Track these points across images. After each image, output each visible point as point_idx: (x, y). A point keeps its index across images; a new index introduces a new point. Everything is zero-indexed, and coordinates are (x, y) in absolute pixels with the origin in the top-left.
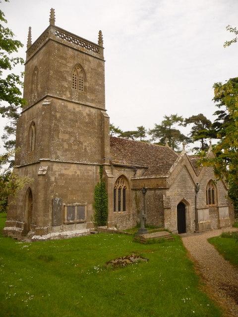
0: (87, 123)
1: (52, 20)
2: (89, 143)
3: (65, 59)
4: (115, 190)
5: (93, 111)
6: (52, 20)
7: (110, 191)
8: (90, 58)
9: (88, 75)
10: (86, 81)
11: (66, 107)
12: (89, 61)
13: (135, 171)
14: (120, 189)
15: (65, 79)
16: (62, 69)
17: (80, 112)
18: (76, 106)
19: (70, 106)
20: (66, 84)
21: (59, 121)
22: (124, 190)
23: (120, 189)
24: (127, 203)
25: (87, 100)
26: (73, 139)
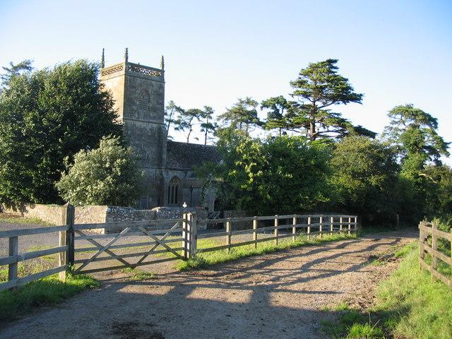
0: (150, 136)
1: (127, 58)
2: (151, 152)
3: (134, 87)
4: (169, 188)
5: (155, 126)
6: (127, 58)
7: (166, 188)
8: (153, 83)
9: (152, 97)
10: (149, 102)
11: (135, 125)
12: (153, 86)
13: (186, 173)
14: (173, 187)
15: (134, 104)
16: (132, 97)
17: (145, 129)
18: (142, 124)
19: (138, 124)
20: (135, 108)
21: (130, 137)
22: (177, 188)
23: (173, 187)
24: (178, 198)
25: (150, 118)
26: (139, 149)
